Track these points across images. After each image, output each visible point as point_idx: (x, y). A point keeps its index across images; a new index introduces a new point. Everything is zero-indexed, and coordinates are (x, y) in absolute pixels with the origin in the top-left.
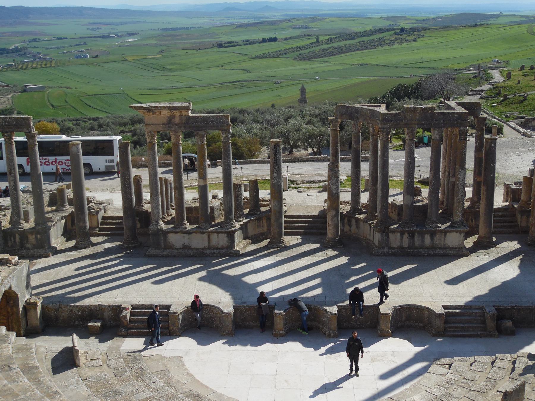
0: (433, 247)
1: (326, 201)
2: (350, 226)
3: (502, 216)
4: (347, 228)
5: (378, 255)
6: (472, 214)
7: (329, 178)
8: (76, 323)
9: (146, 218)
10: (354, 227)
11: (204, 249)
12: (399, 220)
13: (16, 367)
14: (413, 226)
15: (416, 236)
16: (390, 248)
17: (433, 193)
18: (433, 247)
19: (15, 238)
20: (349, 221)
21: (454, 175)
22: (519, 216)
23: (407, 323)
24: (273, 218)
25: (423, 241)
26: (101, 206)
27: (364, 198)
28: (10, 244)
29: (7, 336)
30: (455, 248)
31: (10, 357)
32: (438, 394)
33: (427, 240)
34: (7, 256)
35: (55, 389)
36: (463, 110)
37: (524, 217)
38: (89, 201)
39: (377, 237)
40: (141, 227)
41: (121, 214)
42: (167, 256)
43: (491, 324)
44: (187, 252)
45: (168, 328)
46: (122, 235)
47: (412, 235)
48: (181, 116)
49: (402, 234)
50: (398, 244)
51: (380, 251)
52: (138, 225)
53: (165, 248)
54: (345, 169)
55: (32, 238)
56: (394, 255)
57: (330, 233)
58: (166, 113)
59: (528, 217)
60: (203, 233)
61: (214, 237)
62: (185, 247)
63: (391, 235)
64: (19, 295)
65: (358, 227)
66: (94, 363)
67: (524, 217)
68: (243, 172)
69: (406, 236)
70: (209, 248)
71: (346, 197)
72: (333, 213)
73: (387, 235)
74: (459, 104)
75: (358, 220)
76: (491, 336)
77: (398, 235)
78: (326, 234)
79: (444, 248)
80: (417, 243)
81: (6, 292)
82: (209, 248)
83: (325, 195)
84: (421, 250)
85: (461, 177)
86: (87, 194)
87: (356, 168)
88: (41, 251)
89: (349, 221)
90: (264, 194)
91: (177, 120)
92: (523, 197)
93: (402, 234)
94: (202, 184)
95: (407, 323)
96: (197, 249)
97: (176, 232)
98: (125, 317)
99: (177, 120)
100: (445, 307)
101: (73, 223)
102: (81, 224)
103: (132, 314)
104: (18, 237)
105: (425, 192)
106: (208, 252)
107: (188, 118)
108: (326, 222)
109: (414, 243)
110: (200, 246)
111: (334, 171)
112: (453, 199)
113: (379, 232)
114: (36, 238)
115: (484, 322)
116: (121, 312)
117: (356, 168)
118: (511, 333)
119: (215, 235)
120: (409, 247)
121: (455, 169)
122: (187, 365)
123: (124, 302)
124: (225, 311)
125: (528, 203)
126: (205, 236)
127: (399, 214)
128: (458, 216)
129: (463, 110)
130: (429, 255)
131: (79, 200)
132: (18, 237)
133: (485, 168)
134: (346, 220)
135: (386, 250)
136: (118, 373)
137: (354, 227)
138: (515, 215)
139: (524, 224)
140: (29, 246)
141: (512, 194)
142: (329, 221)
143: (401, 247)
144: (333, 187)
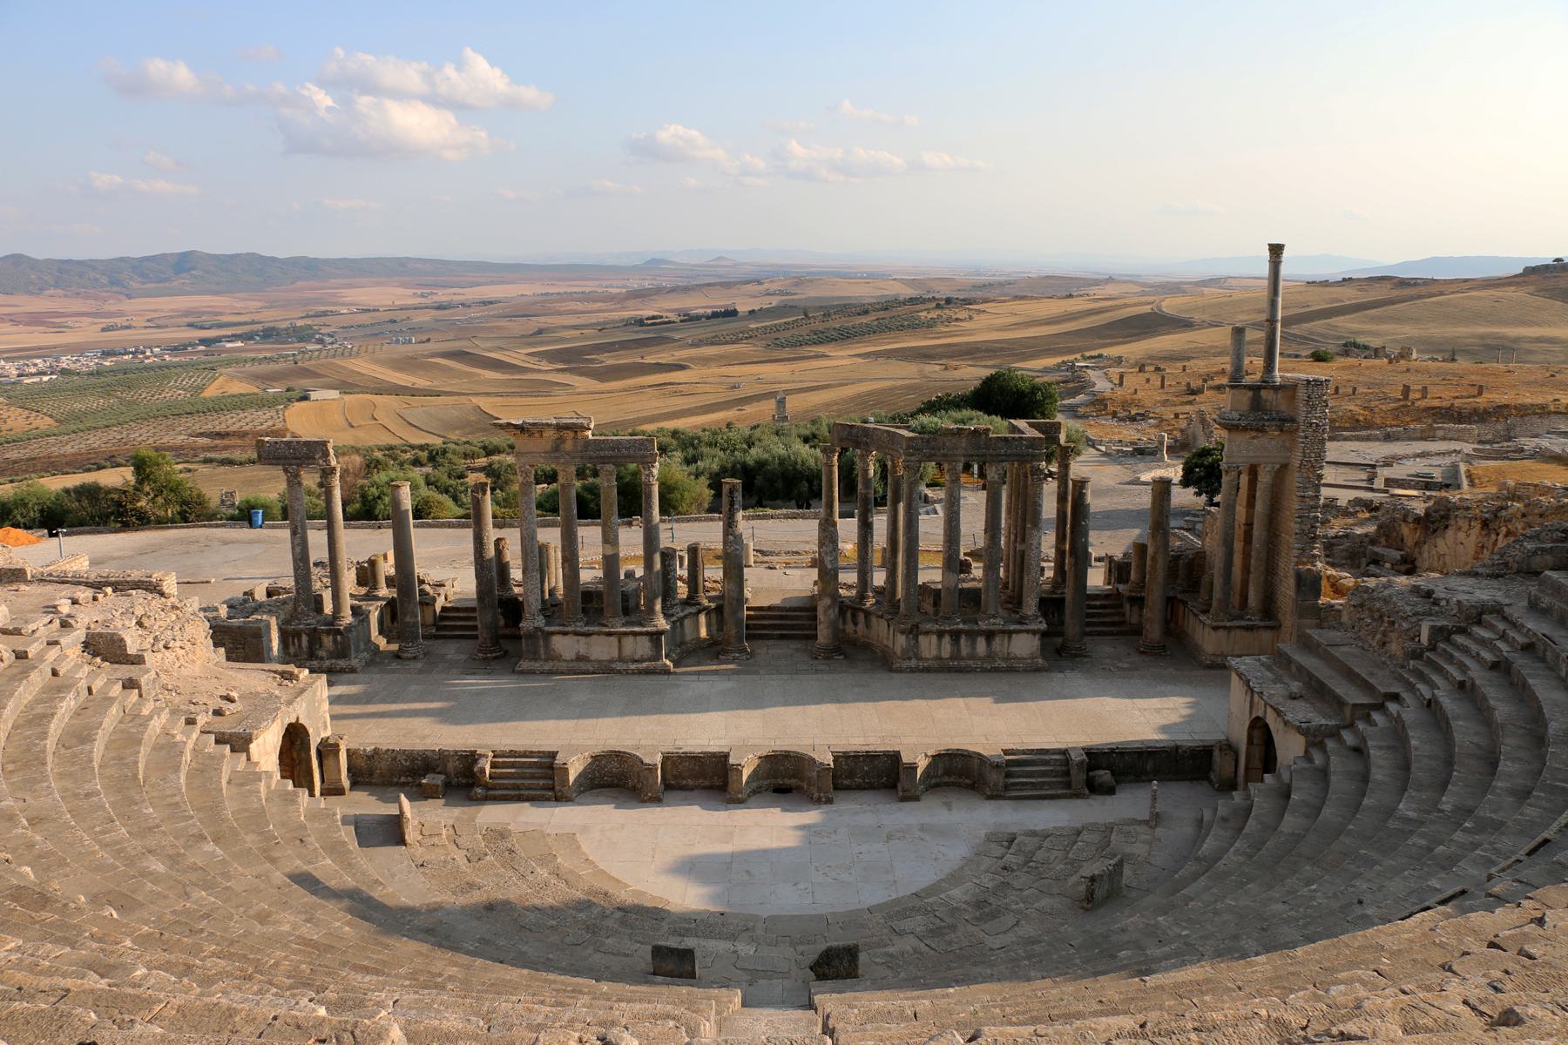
0: (990, 656)
1: (815, 583)
2: (856, 624)
3: (1102, 607)
4: (850, 628)
5: (900, 671)
6: (1051, 605)
7: (821, 544)
8: (403, 779)
9: (513, 609)
10: (861, 627)
12: (936, 613)
13: (313, 841)
16: (920, 659)
17: (991, 569)
19: (300, 641)
20: (854, 616)
21: (1023, 540)
22: (1128, 606)
23: (946, 779)
24: (727, 611)
25: (974, 648)
26: (441, 590)
27: (879, 578)
28: (292, 650)
29: (296, 795)
31: (303, 827)
32: (990, 885)
33: (981, 645)
34: (291, 668)
35: (376, 876)
36: (1037, 434)
37: (1135, 609)
38: (422, 582)
39: (901, 640)
40: (507, 625)
41: (474, 604)
43: (1078, 777)
44: (583, 666)
45: (553, 789)
46: (476, 637)
47: (956, 636)
48: (575, 438)
49: (940, 634)
50: (934, 653)
51: (905, 664)
52: (502, 622)
53: (546, 660)
54: (848, 528)
55: (328, 641)
56: (928, 670)
57: (823, 634)
58: (550, 434)
59: (1141, 608)
60: (609, 634)
61: (628, 642)
62: (580, 658)
63: (921, 638)
64: (311, 731)
65: (868, 626)
66: (435, 840)
67: (1135, 609)
68: (678, 535)
69: (947, 639)
70: (621, 659)
71: (849, 577)
72: (828, 601)
73: (916, 638)
74: (1031, 425)
75: (867, 614)
76: (1077, 796)
77: (934, 638)
78: (815, 637)
79: (1007, 658)
80: (965, 650)
81: (290, 725)
82: (621, 659)
83: (814, 574)
85: (1035, 542)
86: (419, 570)
87: (866, 528)
88: (342, 663)
89: (854, 616)
90: (713, 573)
91: (568, 446)
92: (1133, 576)
93: (940, 634)
94: (610, 552)
95: (946, 779)
96: (599, 661)
97: (565, 634)
98: (483, 771)
100: (1006, 752)
101: (394, 617)
102: (408, 619)
103: (493, 765)
104: (305, 639)
105: (977, 571)
106: (619, 666)
107: (587, 443)
108: (815, 618)
109: (959, 650)
110: (605, 657)
111: (828, 535)
112: (1021, 578)
113: (902, 633)
114: (335, 641)
115: (1067, 773)
116: (475, 761)
117: (866, 528)
118: (1110, 791)
119: (631, 638)
120: (952, 658)
121: (1024, 528)
122: (584, 848)
123: (481, 747)
124: (646, 761)
125: (1141, 584)
126: (614, 639)
127: (936, 604)
128: (1031, 606)
129: (1037, 434)
130: (984, 670)
131: (404, 577)
132: (305, 639)
133: (1073, 527)
134: (849, 615)
135: (913, 663)
136: (474, 858)
137: (861, 627)
138: (1121, 606)
139: (1134, 620)
140: (321, 653)
141: (1119, 571)
142: (821, 616)
143: (939, 658)
144: (828, 559)
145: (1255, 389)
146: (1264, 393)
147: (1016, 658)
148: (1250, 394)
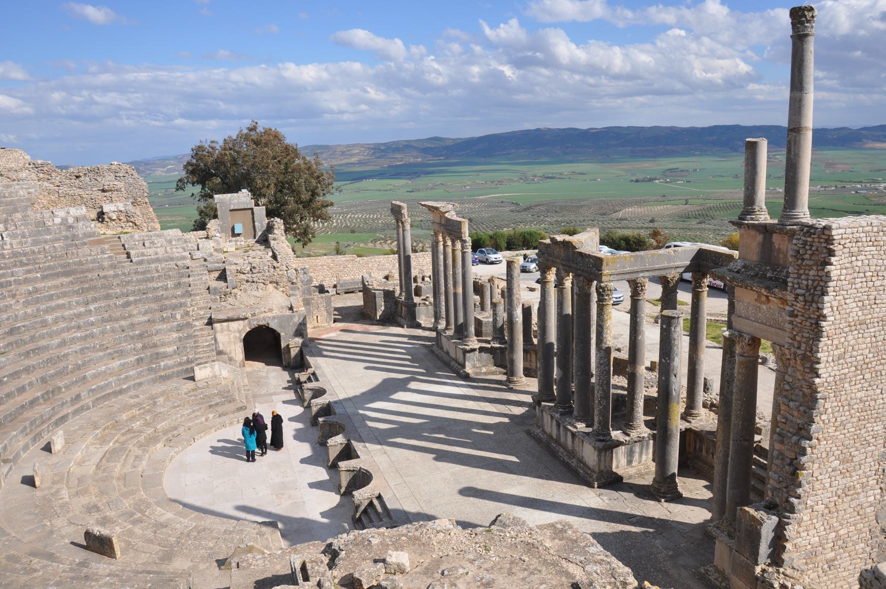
11: (454, 360)
14: (557, 412)
15: (561, 428)
16: (544, 431)
18: (572, 454)
30: (589, 469)
42: (437, 356)
47: (558, 425)
56: (538, 440)
69: (554, 423)
73: (542, 411)
79: (581, 461)
80: (562, 439)
82: (456, 361)
84: (561, 450)
93: (552, 418)
99: (443, 222)
106: (453, 363)
107: (448, 220)
143: (551, 436)
145: (765, 229)
146: (776, 239)
147: (585, 464)
148: (760, 238)
